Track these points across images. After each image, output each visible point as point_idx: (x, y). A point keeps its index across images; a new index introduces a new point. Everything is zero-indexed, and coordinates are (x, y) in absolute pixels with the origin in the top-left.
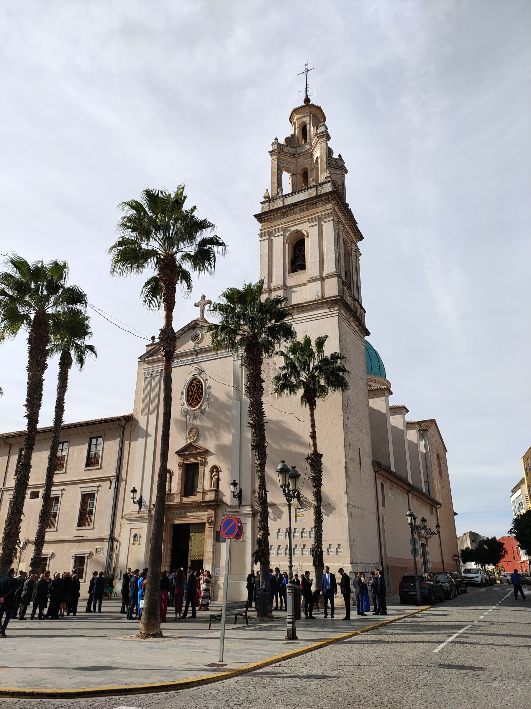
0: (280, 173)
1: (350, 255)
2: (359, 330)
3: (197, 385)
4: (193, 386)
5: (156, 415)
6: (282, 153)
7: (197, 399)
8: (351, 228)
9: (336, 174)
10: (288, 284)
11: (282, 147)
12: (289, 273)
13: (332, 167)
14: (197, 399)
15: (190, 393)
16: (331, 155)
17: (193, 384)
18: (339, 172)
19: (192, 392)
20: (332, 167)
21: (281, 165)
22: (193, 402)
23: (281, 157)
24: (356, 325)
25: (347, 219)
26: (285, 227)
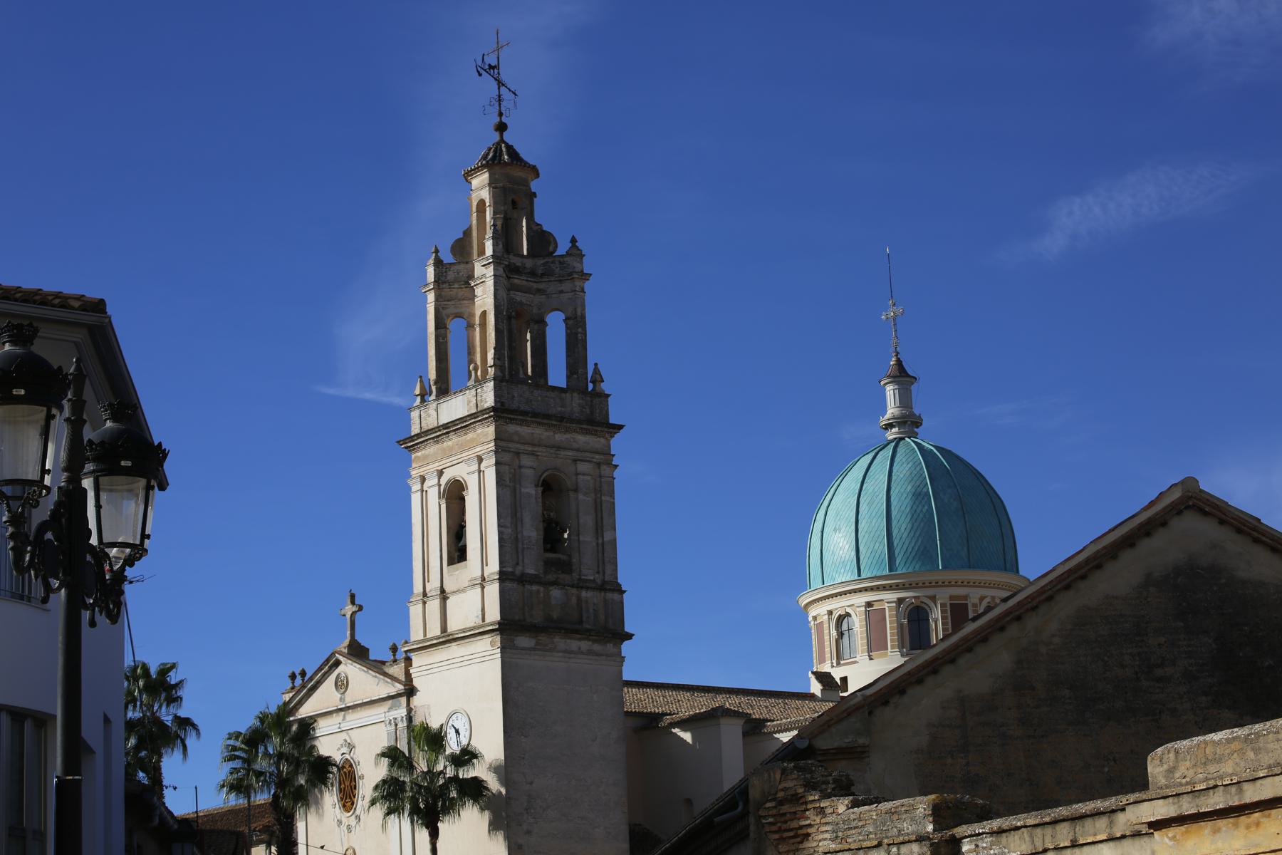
0: (442, 331)
1: (572, 494)
2: (594, 641)
3: (349, 772)
4: (345, 773)
5: (304, 823)
6: (444, 286)
7: (350, 798)
8: (574, 431)
9: (562, 292)
10: (448, 588)
11: (444, 270)
12: (451, 562)
13: (551, 281)
14: (350, 798)
15: (343, 786)
16: (551, 249)
17: (345, 770)
18: (567, 286)
19: (345, 785)
20: (551, 281)
21: (444, 312)
22: (347, 802)
23: (443, 293)
24: (580, 639)
25: (553, 425)
26: (440, 468)
